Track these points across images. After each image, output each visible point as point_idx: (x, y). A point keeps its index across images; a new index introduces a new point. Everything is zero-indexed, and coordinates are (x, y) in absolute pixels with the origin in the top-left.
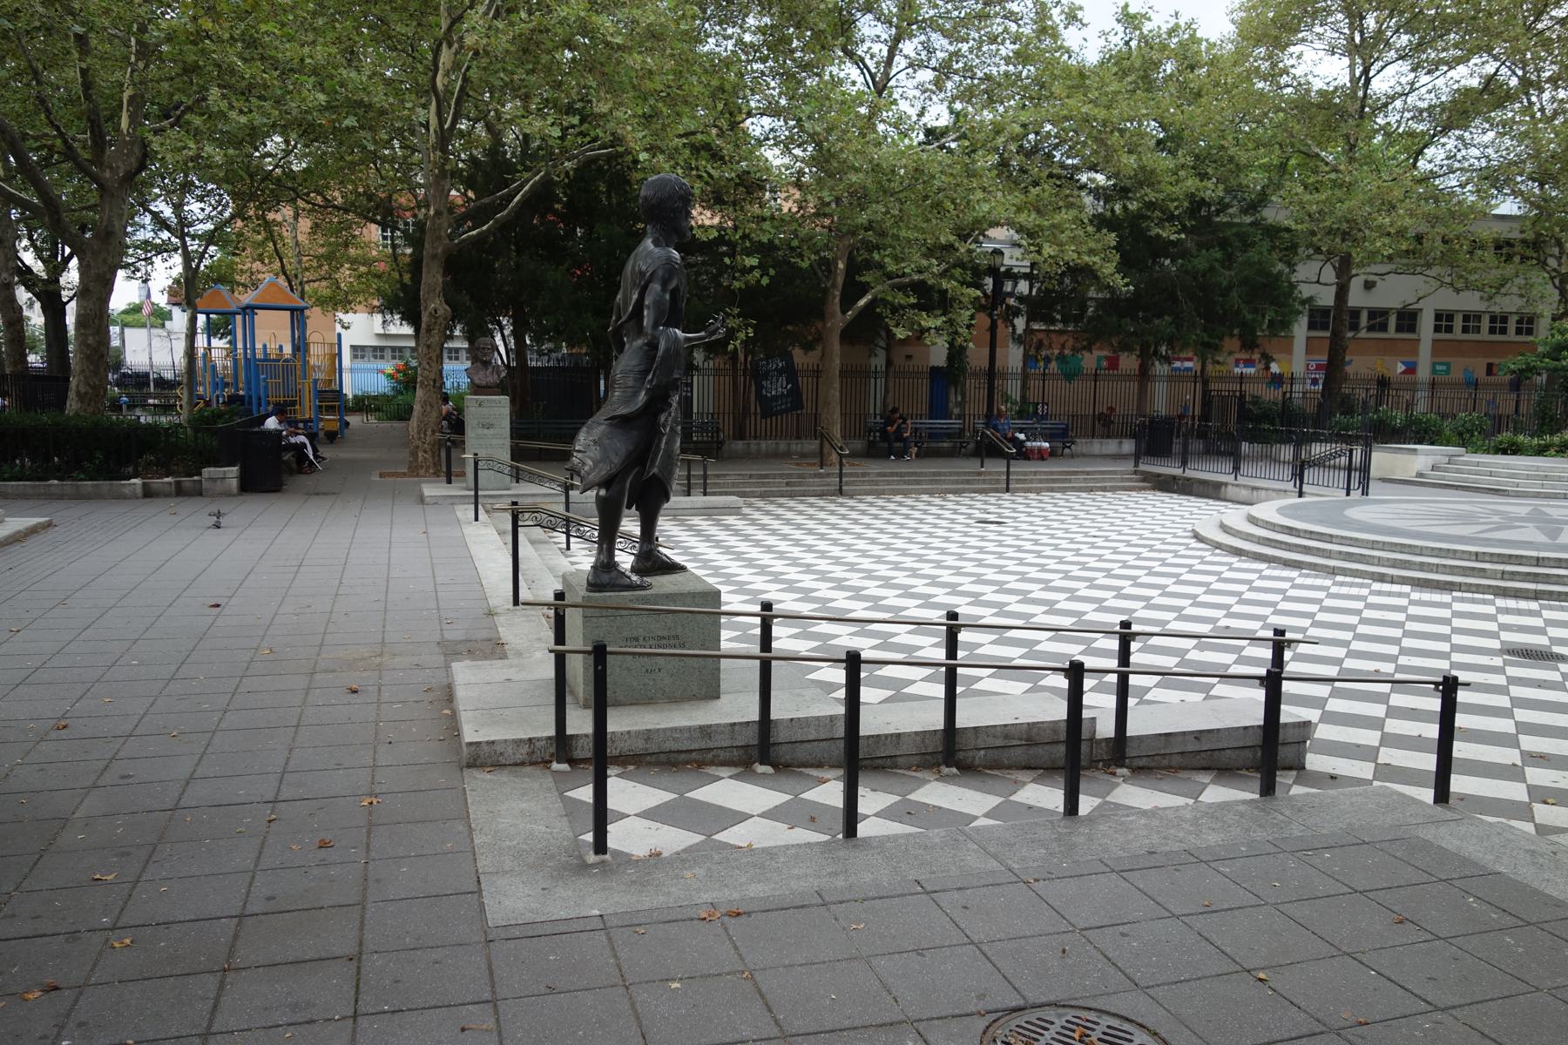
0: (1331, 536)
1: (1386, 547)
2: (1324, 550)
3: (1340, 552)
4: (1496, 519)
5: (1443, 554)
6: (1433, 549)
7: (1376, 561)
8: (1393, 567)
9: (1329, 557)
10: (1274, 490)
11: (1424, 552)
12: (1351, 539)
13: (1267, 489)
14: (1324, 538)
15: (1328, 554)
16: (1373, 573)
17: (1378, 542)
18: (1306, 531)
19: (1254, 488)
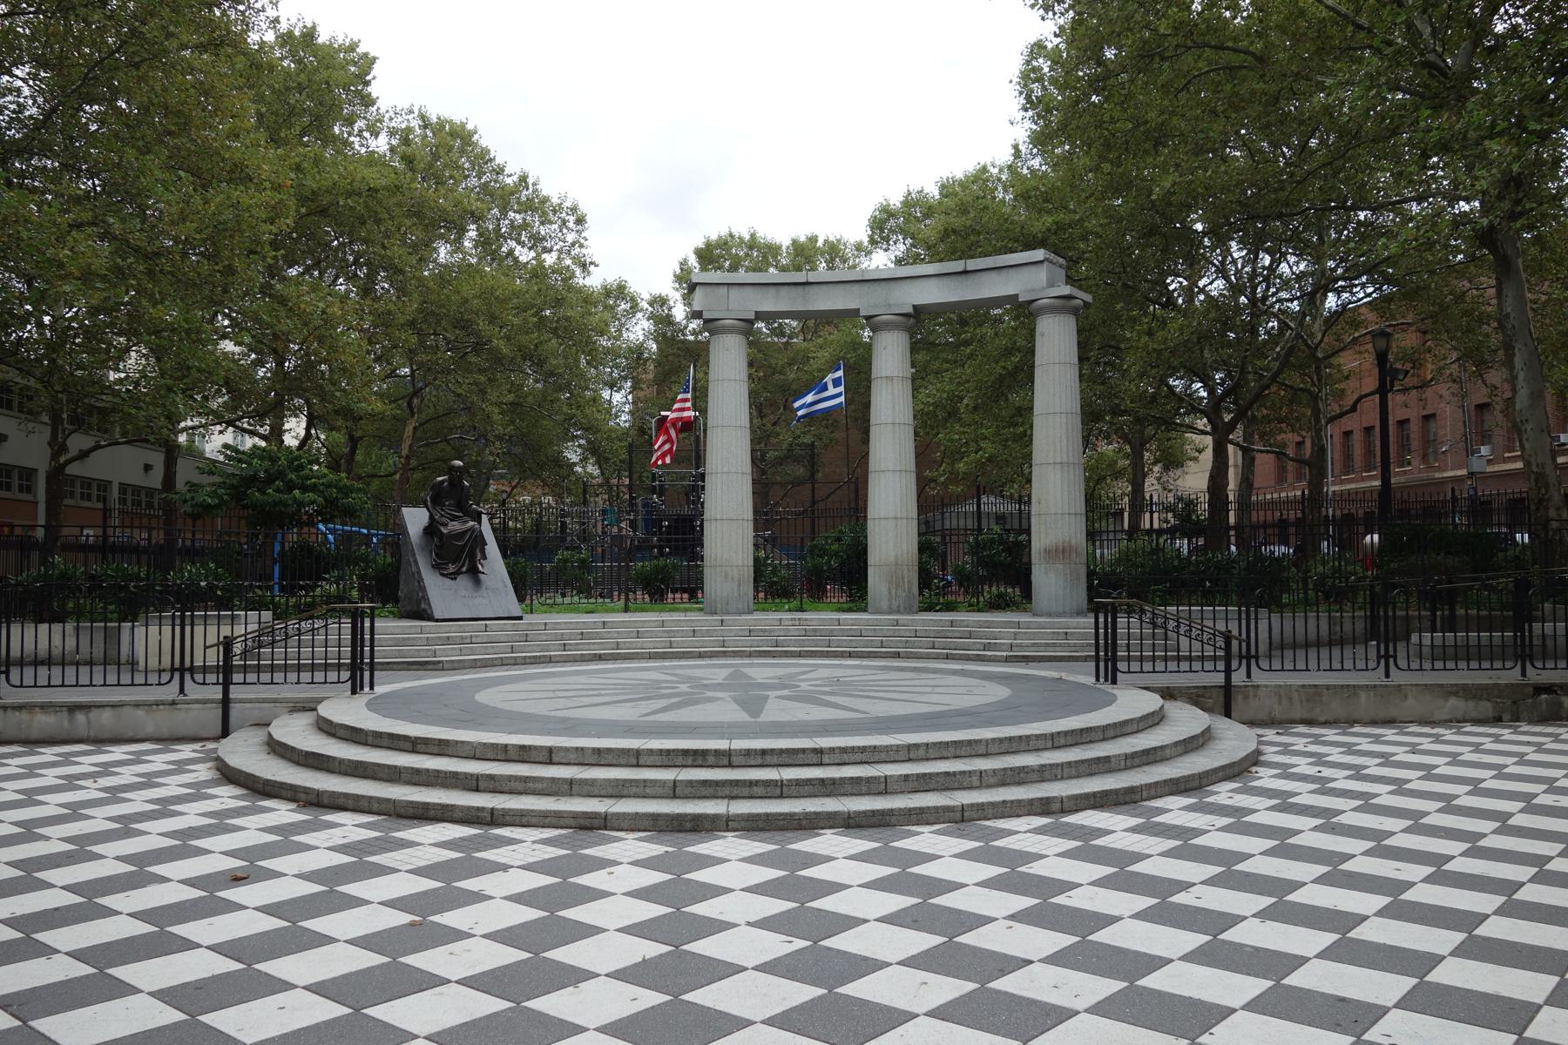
0: (819, 751)
1: (932, 753)
2: (869, 780)
3: (906, 777)
4: (684, 687)
5: (1015, 746)
6: (1001, 740)
7: (975, 781)
8: (1003, 784)
9: (885, 792)
10: (137, 705)
11: (992, 749)
12: (863, 749)
13: (114, 706)
14: (800, 758)
15: (883, 787)
16: (1031, 802)
17: (917, 746)
18: (748, 753)
19: (73, 708)
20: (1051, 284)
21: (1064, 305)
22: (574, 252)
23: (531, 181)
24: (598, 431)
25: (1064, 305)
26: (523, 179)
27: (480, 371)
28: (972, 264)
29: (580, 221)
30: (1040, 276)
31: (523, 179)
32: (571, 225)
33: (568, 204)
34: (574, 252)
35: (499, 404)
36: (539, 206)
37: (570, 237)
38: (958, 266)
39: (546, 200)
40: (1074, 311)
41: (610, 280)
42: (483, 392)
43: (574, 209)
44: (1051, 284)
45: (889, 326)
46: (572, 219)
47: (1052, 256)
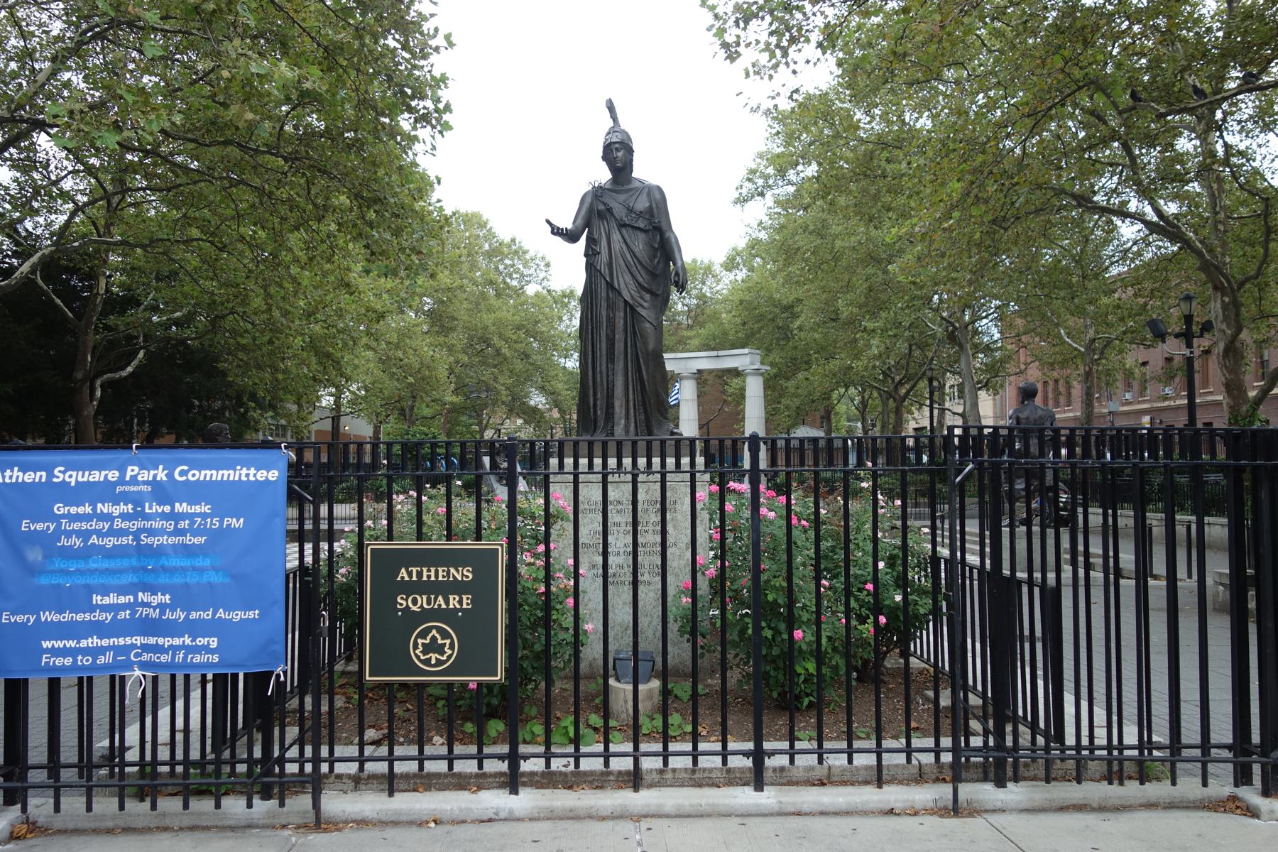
20: (752, 364)
21: (757, 372)
22: (545, 284)
23: (517, 241)
24: (559, 394)
25: (757, 372)
26: (513, 240)
27: (495, 367)
28: (721, 353)
29: (548, 265)
30: (747, 360)
31: (513, 240)
32: (542, 268)
33: (540, 255)
34: (545, 284)
35: (503, 385)
36: (519, 253)
37: (542, 275)
38: (714, 353)
39: (525, 252)
40: (762, 374)
41: (565, 287)
42: (495, 380)
43: (543, 258)
44: (752, 364)
45: (686, 378)
46: (543, 264)
47: (753, 351)
